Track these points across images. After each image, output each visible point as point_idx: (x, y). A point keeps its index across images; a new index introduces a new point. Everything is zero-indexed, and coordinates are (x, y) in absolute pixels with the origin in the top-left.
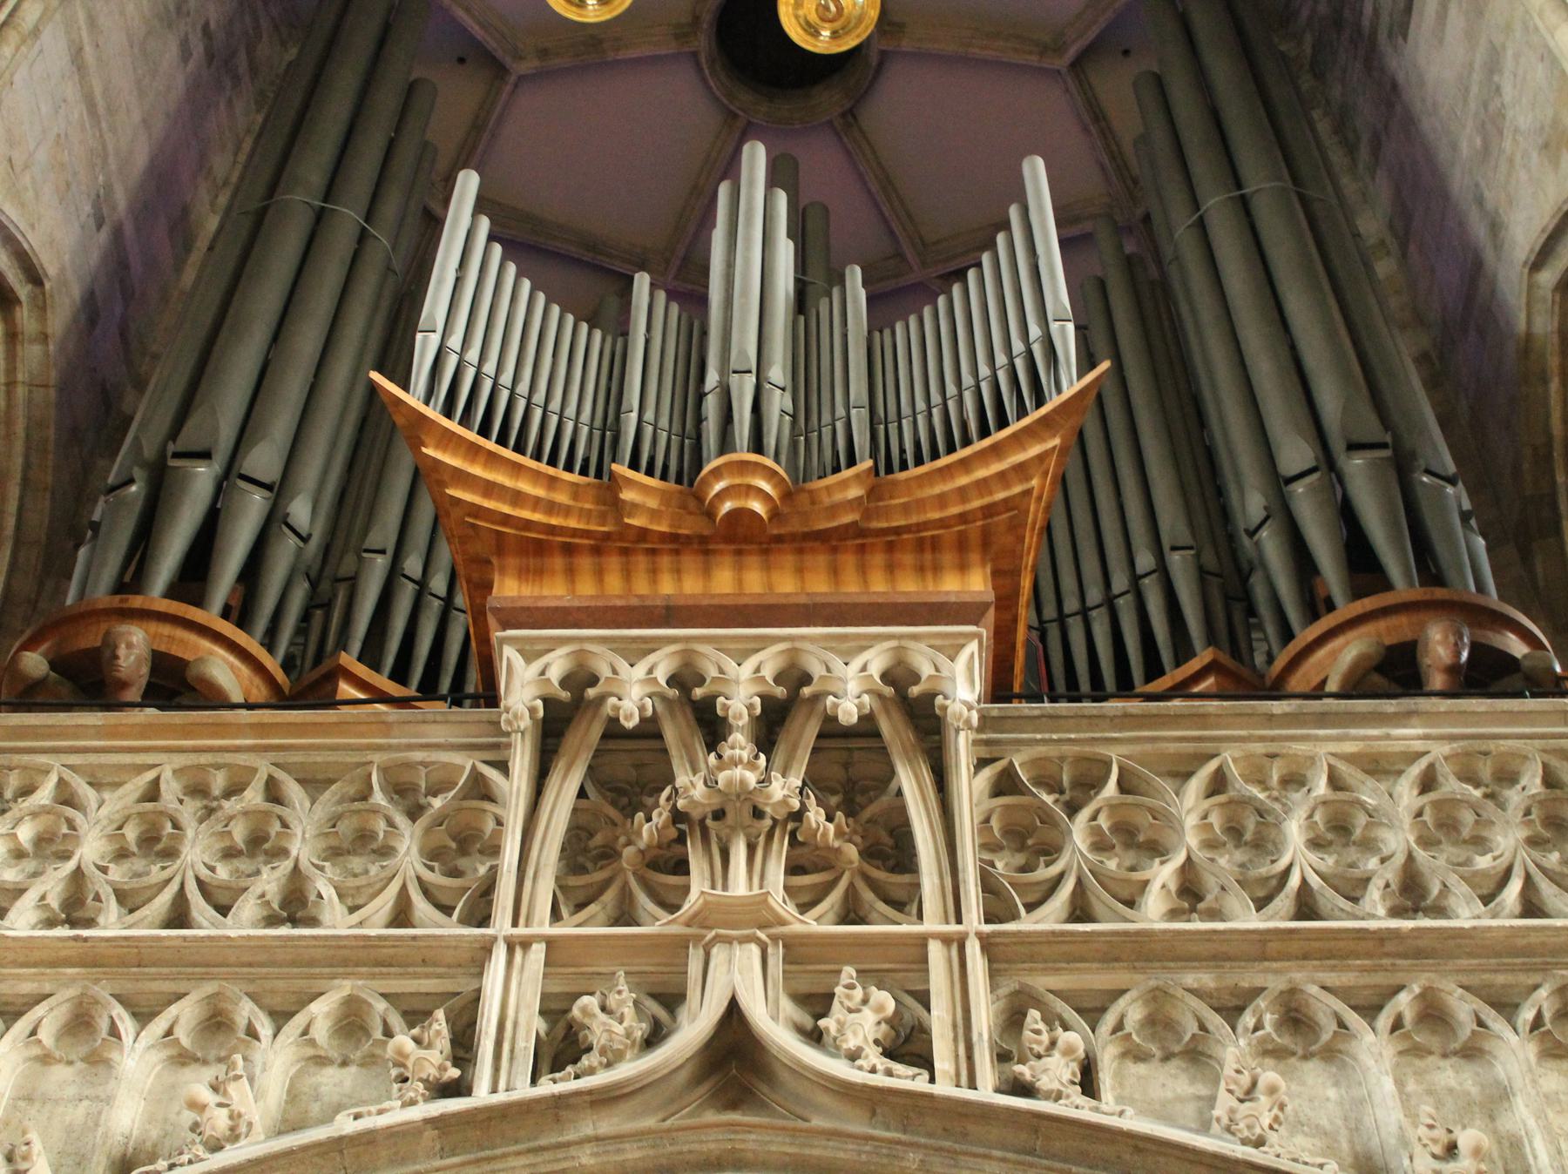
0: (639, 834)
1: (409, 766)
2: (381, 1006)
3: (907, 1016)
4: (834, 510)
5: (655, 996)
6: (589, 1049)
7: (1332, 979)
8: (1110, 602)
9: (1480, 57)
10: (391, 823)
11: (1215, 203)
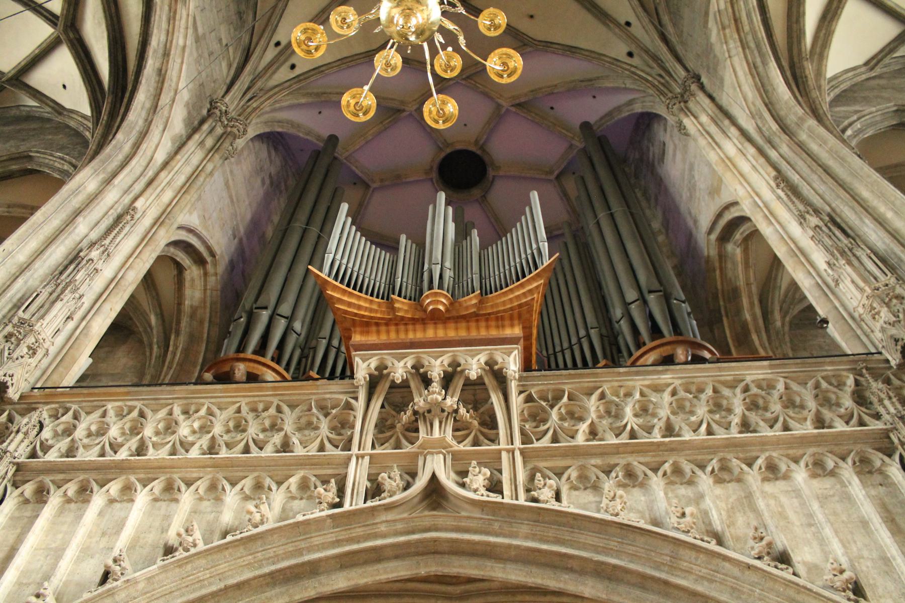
0: (402, 419)
1: (325, 399)
2: (313, 479)
3: (495, 478)
4: (467, 308)
5: (408, 473)
6: (384, 491)
7: (642, 459)
8: (571, 347)
9: (687, 167)
10: (318, 419)
11: (602, 215)
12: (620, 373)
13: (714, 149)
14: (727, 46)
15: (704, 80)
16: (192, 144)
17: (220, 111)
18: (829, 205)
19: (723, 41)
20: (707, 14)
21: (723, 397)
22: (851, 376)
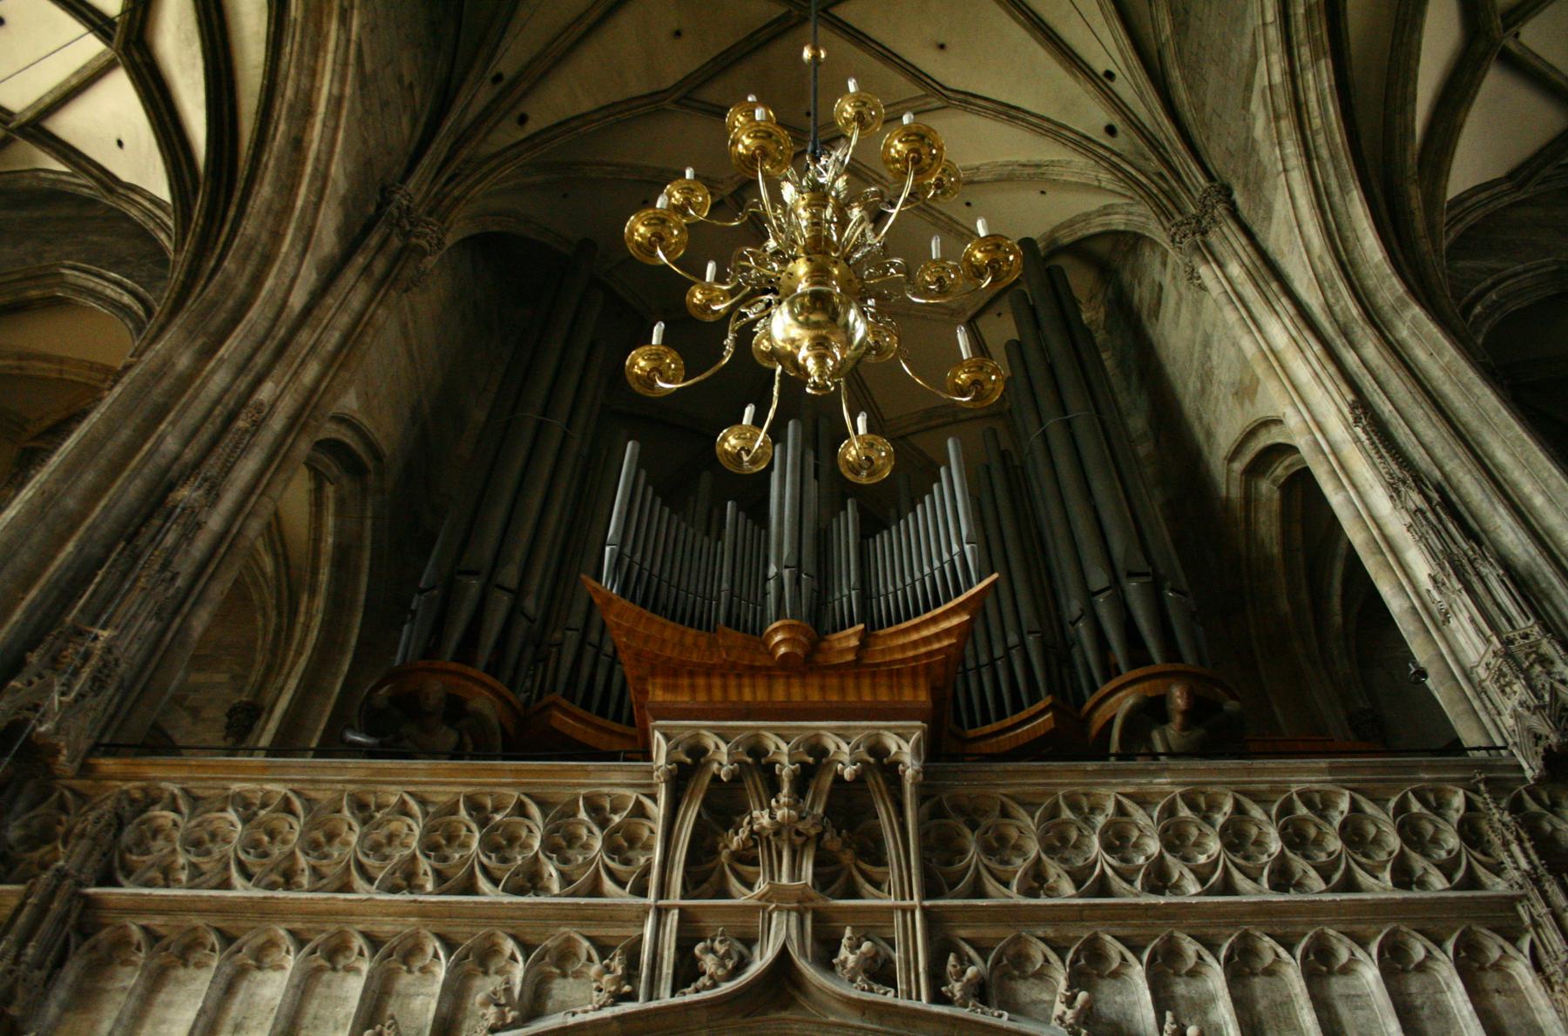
0: (731, 841)
1: (601, 795)
2: (586, 944)
3: (882, 952)
4: (843, 651)
5: (741, 940)
6: (704, 973)
8: (992, 662)
9: (1199, 338)
10: (590, 831)
11: (1052, 422)
12: (1086, 772)
13: (1251, 332)
14: (1281, 150)
15: (1239, 197)
16: (350, 275)
17: (398, 208)
18: (1441, 469)
19: (1276, 141)
20: (1249, 87)
21: (1252, 820)
22: (1461, 792)
